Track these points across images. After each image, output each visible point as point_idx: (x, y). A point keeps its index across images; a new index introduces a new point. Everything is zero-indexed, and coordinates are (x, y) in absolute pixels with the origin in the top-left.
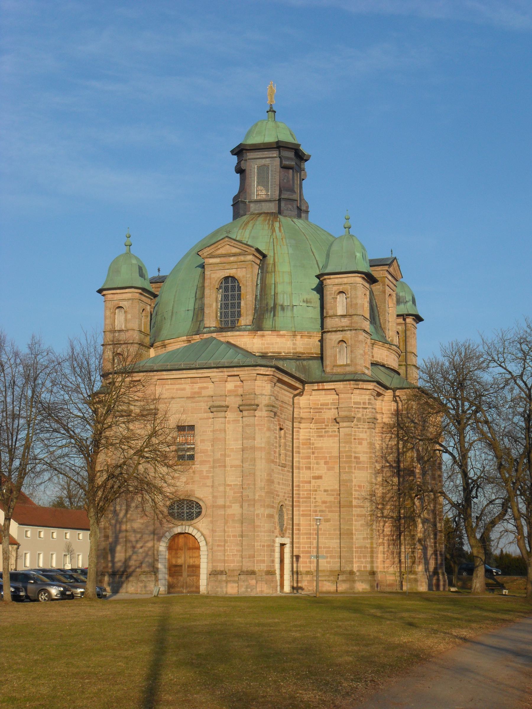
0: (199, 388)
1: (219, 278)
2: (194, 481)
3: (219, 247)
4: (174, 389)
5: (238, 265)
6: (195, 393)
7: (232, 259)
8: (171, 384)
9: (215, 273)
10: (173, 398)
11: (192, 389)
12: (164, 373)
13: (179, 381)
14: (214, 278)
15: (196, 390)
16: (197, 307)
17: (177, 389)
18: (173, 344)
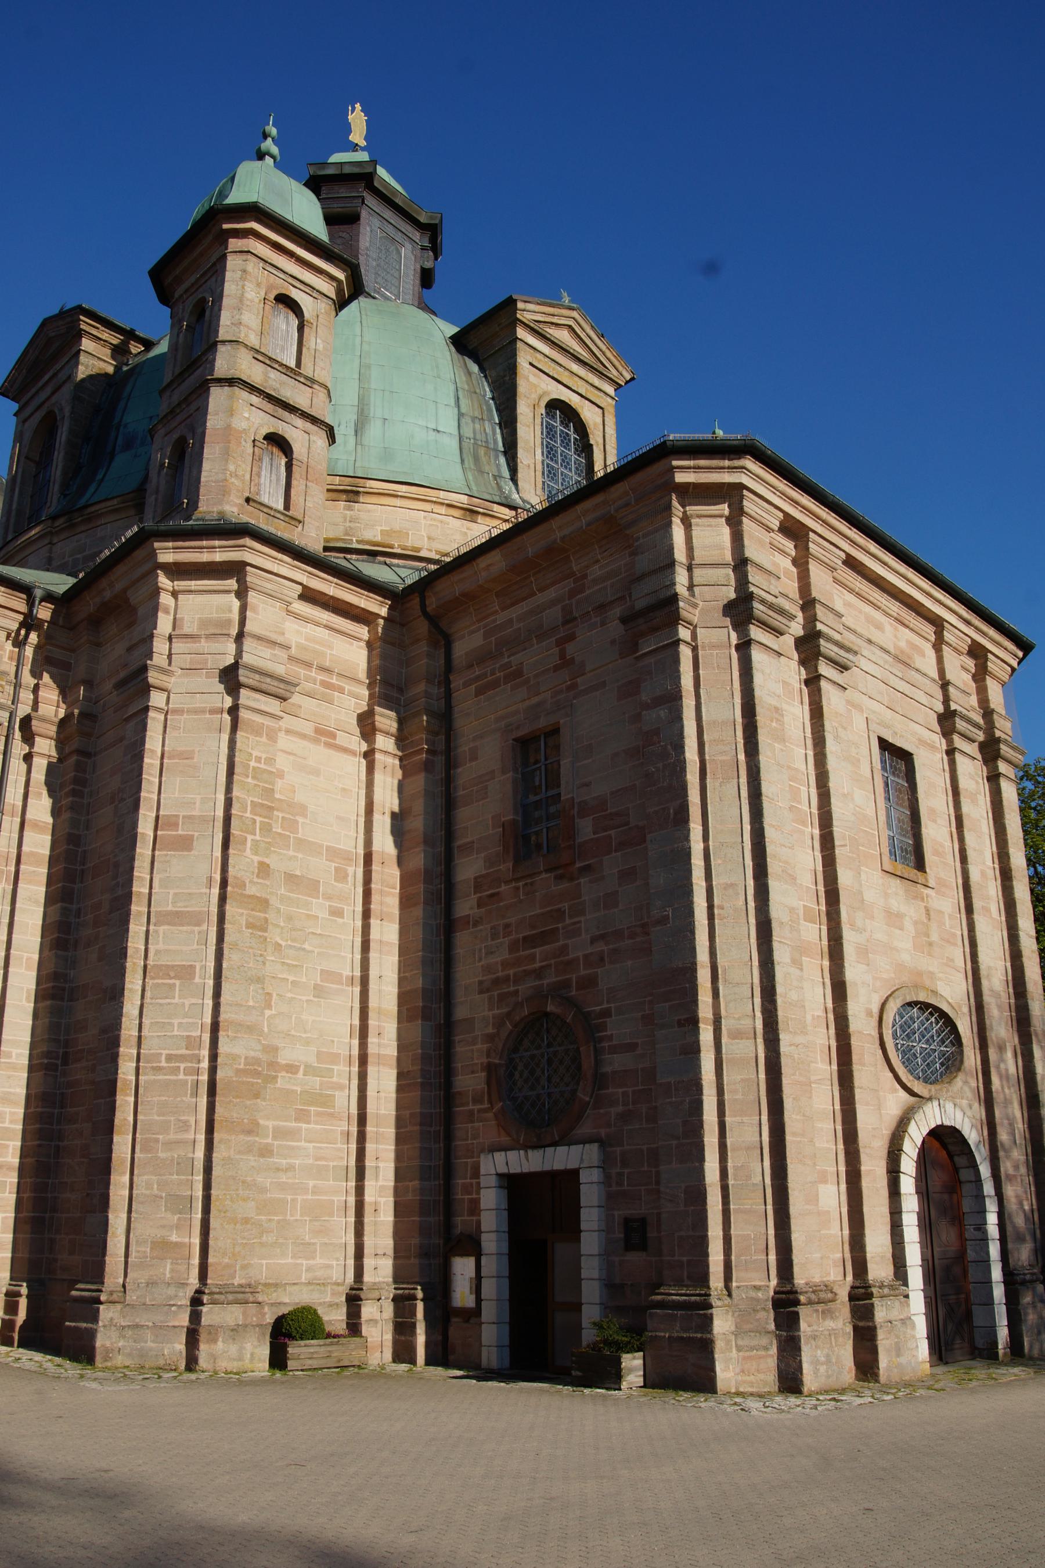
0: (908, 642)
1: (545, 393)
2: (930, 944)
3: (555, 320)
4: (860, 612)
5: (587, 390)
6: (902, 652)
7: (575, 367)
8: (859, 595)
9: (539, 377)
10: (870, 641)
11: (896, 637)
12: (873, 547)
13: (876, 595)
14: (535, 386)
15: (903, 644)
16: (468, 432)
17: (869, 620)
18: (398, 502)
